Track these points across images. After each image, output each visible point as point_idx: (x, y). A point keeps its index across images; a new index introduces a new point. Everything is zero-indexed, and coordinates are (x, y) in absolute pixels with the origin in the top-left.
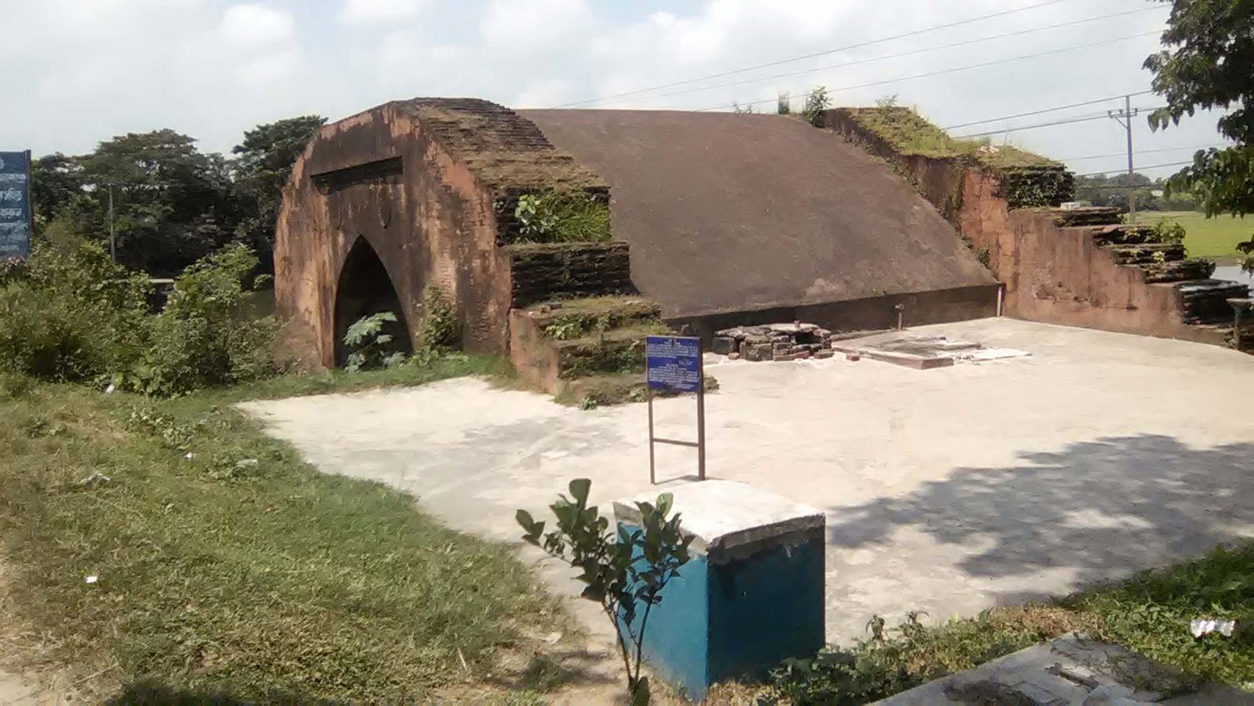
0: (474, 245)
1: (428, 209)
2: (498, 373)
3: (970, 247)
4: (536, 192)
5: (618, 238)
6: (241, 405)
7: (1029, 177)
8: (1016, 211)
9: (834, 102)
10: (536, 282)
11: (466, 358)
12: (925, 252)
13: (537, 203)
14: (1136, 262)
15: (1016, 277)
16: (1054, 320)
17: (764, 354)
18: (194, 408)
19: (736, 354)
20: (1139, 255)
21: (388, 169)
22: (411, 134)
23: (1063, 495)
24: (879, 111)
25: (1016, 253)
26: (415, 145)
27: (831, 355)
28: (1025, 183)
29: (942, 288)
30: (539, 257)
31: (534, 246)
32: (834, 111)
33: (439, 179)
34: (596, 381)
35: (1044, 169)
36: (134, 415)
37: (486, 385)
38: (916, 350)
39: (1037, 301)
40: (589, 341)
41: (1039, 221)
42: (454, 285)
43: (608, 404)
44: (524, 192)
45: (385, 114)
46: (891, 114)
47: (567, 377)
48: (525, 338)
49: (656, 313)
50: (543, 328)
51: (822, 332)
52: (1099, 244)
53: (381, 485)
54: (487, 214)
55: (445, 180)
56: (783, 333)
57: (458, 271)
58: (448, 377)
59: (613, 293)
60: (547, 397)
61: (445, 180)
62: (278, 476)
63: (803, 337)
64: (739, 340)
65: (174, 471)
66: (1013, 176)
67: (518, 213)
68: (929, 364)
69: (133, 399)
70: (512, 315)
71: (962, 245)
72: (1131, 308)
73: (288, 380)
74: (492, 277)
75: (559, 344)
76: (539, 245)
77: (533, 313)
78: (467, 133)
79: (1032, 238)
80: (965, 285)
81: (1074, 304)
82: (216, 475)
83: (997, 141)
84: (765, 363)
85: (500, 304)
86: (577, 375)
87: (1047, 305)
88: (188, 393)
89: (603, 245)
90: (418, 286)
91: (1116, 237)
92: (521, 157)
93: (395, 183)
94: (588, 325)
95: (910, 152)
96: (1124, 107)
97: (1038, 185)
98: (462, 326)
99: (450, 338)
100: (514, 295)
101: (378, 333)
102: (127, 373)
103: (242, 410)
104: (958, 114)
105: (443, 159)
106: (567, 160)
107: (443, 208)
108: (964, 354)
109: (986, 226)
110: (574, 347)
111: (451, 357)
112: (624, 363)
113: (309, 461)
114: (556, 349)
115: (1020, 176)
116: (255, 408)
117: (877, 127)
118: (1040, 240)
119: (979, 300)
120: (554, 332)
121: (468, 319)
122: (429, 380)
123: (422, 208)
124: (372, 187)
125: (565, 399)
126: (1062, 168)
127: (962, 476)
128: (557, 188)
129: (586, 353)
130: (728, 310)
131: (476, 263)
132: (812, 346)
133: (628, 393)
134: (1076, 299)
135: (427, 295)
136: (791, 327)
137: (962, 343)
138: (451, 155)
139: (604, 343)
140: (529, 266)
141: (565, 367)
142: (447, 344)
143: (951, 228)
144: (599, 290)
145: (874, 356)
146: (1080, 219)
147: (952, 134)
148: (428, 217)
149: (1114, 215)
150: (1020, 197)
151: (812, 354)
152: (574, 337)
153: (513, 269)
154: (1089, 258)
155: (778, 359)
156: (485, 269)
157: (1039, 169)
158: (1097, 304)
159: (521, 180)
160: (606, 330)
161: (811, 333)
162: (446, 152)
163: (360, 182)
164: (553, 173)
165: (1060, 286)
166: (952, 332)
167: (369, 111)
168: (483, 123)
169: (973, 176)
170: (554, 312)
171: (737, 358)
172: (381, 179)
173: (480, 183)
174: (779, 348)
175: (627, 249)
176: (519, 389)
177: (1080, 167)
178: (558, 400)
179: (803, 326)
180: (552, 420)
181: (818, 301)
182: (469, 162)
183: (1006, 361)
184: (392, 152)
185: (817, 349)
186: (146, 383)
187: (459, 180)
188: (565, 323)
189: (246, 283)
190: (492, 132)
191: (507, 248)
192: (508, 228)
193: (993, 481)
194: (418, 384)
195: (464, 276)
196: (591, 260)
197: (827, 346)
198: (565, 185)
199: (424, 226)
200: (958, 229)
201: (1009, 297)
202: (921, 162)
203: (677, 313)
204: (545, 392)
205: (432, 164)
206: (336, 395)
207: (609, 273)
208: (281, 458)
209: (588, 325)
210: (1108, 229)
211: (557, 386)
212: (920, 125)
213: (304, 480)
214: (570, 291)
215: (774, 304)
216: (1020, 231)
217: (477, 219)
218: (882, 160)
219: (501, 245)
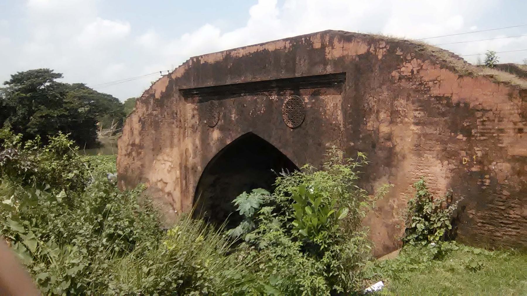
9: (502, 60)
22: (367, 56)
55: (435, 91)
124: (274, 97)
167: (221, 52)
184: (330, 70)
199: (384, 129)
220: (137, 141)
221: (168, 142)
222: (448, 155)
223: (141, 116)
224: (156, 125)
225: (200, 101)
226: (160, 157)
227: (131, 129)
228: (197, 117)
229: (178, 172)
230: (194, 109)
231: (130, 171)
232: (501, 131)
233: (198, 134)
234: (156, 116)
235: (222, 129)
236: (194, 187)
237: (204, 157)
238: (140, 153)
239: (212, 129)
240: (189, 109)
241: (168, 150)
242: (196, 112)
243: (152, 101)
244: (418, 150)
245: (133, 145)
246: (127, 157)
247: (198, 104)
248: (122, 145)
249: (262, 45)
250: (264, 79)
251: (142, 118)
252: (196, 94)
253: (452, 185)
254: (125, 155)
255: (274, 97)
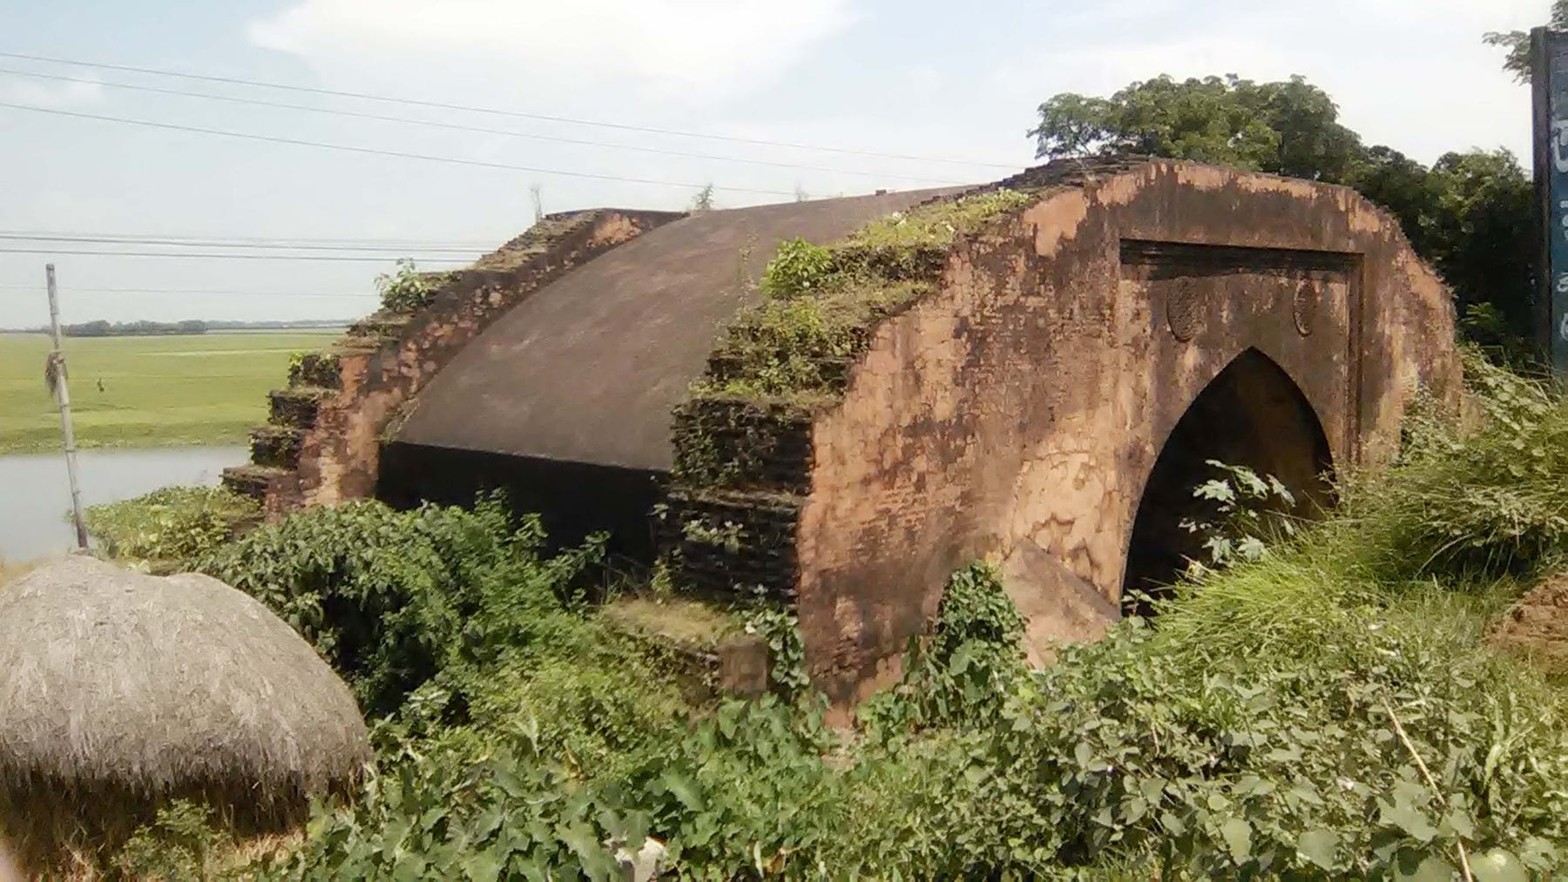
55: (1414, 289)
61: (1414, 289)
131: (1437, 363)
163: (1254, 269)
172: (1300, 273)
184: (1351, 246)
205: (1401, 270)
220: (943, 409)
221: (1080, 396)
223: (966, 312)
224: (1038, 343)
225: (1154, 277)
226: (1048, 447)
227: (910, 365)
228: (1147, 317)
229: (1112, 476)
230: (1139, 296)
231: (898, 536)
233: (1151, 359)
234: (1040, 312)
235: (1203, 344)
236: (1132, 504)
237: (1162, 416)
238: (961, 452)
239: (1183, 345)
241: (1079, 417)
242: (1143, 304)
243: (1021, 264)
244: (1405, 352)
245: (918, 428)
246: (876, 487)
247: (1150, 283)
248: (845, 441)
250: (1287, 246)
251: (971, 320)
252: (1151, 257)
254: (866, 481)
255: (1284, 281)
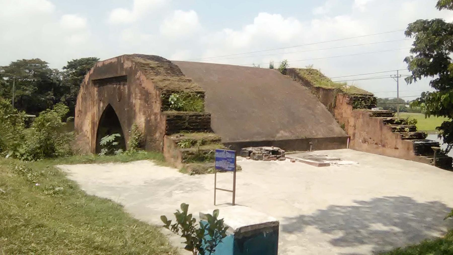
0: (152, 110)
1: (136, 96)
2: (158, 159)
3: (338, 122)
4: (178, 92)
5: (207, 111)
6: (58, 166)
7: (360, 98)
8: (355, 110)
10: (175, 126)
11: (146, 153)
12: (321, 123)
13: (178, 96)
14: (399, 132)
15: (354, 135)
16: (367, 151)
17: (260, 158)
18: (41, 166)
19: (249, 157)
20: (400, 129)
21: (122, 79)
22: (131, 68)
23: (368, 217)
24: (307, 70)
25: (355, 126)
26: (132, 72)
27: (285, 160)
28: (359, 100)
29: (327, 137)
30: (177, 116)
31: (175, 112)
32: (290, 69)
33: (141, 85)
34: (196, 165)
35: (366, 95)
36: (16, 167)
37: (153, 164)
38: (316, 160)
39: (362, 144)
40: (194, 149)
41: (363, 114)
42: (144, 125)
43: (199, 174)
44: (173, 92)
45: (122, 59)
46: (311, 71)
47: (185, 162)
48: (170, 147)
49: (219, 140)
50: (177, 143)
51: (282, 151)
52: (385, 124)
53: (110, 200)
54: (158, 99)
55: (143, 85)
56: (267, 150)
57: (145, 120)
58: (139, 160)
59: (204, 132)
60: (176, 170)
61: (143, 85)
62: (71, 194)
63: (274, 152)
64: (250, 152)
65: (30, 190)
66: (355, 97)
67: (170, 100)
68: (321, 165)
69: (17, 161)
70: (165, 138)
71: (335, 121)
72: (396, 148)
73: (78, 158)
74: (158, 123)
75: (183, 150)
76: (177, 112)
77: (173, 137)
78: (152, 68)
79: (361, 120)
80: (335, 136)
81: (376, 146)
82: (46, 193)
83: (350, 84)
84: (260, 161)
85: (161, 133)
86: (188, 162)
87: (365, 145)
88: (38, 160)
89: (201, 113)
90: (130, 125)
91: (391, 122)
92: (172, 78)
93: (124, 85)
94: (194, 143)
95: (317, 86)
96: (396, 74)
97: (363, 101)
98: (146, 140)
99: (141, 145)
100: (167, 130)
101: (113, 141)
102: (15, 150)
103: (58, 168)
104: (336, 73)
105: (143, 78)
106: (190, 81)
107: (141, 95)
108: (334, 162)
109: (344, 115)
110: (188, 151)
111: (140, 152)
112: (206, 158)
113: (83, 189)
114: (181, 152)
115: (357, 97)
116: (64, 168)
117: (305, 76)
118: (364, 121)
119: (341, 142)
120: (181, 145)
121: (148, 138)
122: (132, 160)
123: (134, 95)
124: (115, 86)
125: (183, 171)
126: (373, 95)
127: (332, 208)
128: (186, 91)
129: (192, 154)
130: (248, 140)
131: (153, 117)
132: (278, 156)
133: (207, 170)
134: (376, 144)
135: (133, 128)
136: (270, 148)
137: (333, 158)
138: (146, 76)
139: (199, 151)
140: (172, 120)
141: (184, 159)
142: (140, 147)
143: (331, 115)
144: (198, 130)
145: (300, 161)
146: (379, 114)
147: (333, 80)
148: (135, 99)
149: (391, 114)
150: (357, 105)
151: (278, 158)
152: (188, 147)
153: (167, 120)
154: (381, 129)
155: (264, 160)
156: (156, 120)
157: (364, 95)
158: (384, 146)
159: (172, 87)
160: (200, 145)
161: (278, 151)
162: (144, 75)
164: (184, 85)
165: (370, 138)
166: (330, 154)
168: (159, 65)
169: (340, 97)
170: (181, 138)
171: (249, 159)
172: (119, 83)
173: (157, 88)
174: (265, 156)
175: (210, 115)
176: (166, 166)
177: (379, 95)
178: (180, 171)
179: (275, 148)
180: (178, 179)
181: (281, 139)
182: (152, 79)
183: (350, 166)
184: (124, 74)
185: (279, 157)
186: (22, 155)
187: (148, 86)
188: (185, 142)
189: (64, 120)
190: (162, 69)
191: (165, 112)
192: (166, 105)
193: (343, 210)
194: (127, 162)
195: (148, 122)
196: (196, 119)
197: (283, 156)
198: (188, 90)
199: (134, 102)
200: (334, 115)
201: (351, 141)
202: (321, 90)
203: (228, 140)
204: (176, 168)
206: (95, 164)
207: (203, 124)
208: (72, 188)
209: (194, 143)
210: (389, 118)
211: (180, 166)
212: (321, 76)
213: (80, 197)
214: (187, 130)
215: (264, 139)
216: (356, 117)
217: (154, 100)
218: (307, 88)
219: (162, 111)
222: (144, 114)
232: (153, 102)
240: (95, 90)
249: (111, 59)
253: (145, 126)
255: (115, 86)
